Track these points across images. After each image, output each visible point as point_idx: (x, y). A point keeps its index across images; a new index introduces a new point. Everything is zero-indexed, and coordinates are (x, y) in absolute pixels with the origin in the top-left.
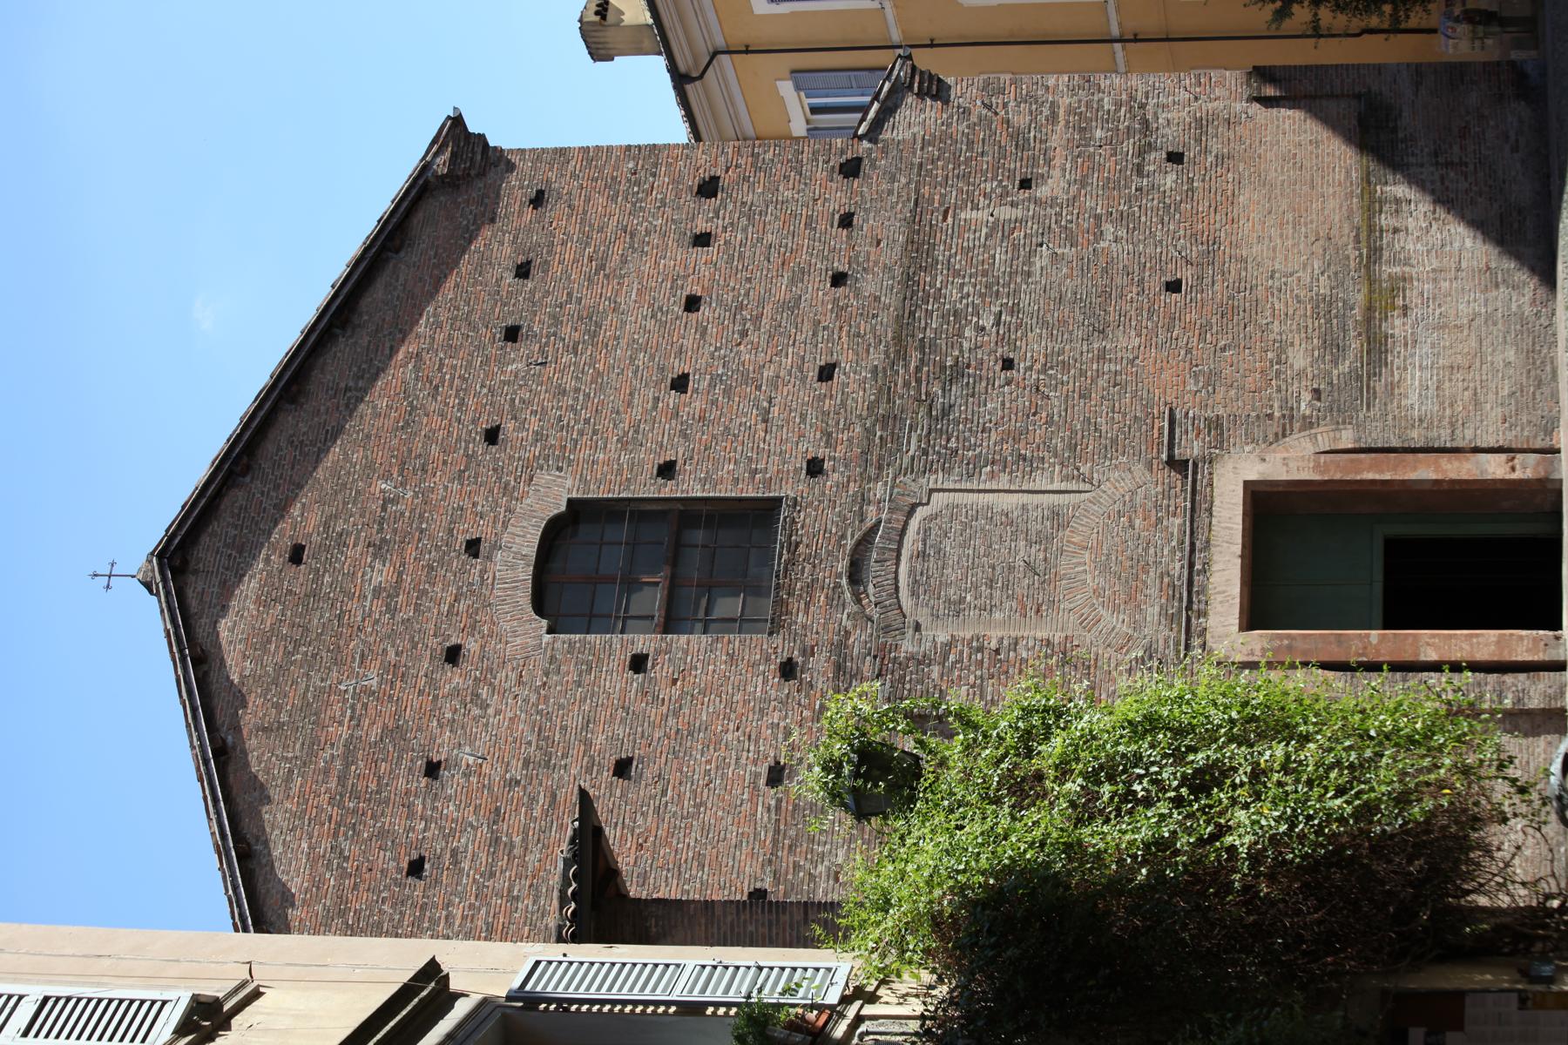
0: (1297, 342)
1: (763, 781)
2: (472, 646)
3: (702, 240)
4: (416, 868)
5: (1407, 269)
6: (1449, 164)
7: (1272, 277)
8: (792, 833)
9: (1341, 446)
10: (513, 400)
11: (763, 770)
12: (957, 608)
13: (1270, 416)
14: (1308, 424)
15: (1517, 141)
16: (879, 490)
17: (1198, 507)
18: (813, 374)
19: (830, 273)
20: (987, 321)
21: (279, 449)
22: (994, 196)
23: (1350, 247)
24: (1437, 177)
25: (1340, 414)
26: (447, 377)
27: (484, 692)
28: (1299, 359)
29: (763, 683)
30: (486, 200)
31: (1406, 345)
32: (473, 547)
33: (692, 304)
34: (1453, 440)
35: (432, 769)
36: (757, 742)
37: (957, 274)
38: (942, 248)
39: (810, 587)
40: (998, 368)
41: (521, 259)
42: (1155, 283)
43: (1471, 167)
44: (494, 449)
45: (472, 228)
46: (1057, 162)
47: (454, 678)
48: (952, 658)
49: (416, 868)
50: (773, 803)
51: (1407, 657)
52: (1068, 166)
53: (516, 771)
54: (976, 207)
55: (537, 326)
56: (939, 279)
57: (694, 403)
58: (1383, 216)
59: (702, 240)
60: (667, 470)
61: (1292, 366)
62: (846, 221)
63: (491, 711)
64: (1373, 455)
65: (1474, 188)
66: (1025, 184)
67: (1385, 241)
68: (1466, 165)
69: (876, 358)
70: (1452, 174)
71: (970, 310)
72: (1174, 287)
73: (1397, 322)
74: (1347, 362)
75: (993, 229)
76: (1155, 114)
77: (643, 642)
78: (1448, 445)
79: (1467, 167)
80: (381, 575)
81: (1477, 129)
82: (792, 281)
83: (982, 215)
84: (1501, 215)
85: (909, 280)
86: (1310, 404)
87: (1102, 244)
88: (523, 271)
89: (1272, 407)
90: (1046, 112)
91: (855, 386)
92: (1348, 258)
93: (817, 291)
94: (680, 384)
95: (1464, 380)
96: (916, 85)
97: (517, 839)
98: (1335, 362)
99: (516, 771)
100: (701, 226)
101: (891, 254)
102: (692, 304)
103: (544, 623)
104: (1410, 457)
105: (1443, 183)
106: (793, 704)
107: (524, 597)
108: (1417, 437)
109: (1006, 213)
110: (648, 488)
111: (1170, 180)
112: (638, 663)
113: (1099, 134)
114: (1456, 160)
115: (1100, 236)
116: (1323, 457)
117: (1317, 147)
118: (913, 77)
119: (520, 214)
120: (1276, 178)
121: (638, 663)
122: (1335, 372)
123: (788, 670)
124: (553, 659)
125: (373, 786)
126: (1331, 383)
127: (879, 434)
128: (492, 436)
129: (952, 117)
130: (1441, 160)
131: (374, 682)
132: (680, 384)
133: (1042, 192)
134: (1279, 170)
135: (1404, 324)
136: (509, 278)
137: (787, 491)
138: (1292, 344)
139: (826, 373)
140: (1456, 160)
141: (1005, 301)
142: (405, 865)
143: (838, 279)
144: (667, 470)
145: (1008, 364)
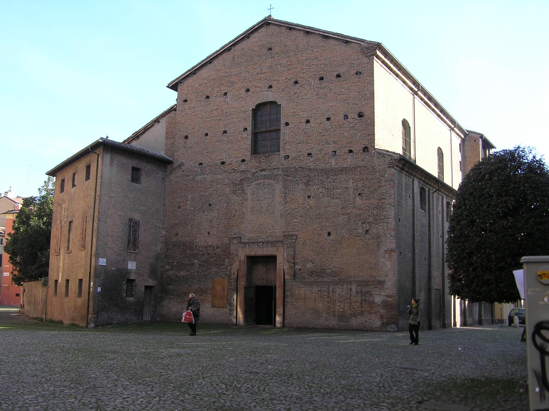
0: (313, 265)
1: (222, 161)
2: (250, 93)
3: (346, 117)
5: (331, 292)
6: (362, 304)
7: (331, 258)
8: (212, 169)
9: (285, 276)
10: (304, 84)
11: (224, 160)
12: (253, 195)
13: (294, 259)
14: (291, 267)
15: (368, 322)
17: (273, 243)
18: (309, 152)
19: (336, 150)
20: (320, 190)
21: (294, 35)
22: (357, 187)
23: (339, 277)
24: (358, 300)
25: (294, 276)
26: (311, 67)
27: (240, 99)
28: (309, 265)
30: (358, 60)
31: (311, 291)
32: (271, 87)
33: (328, 119)
34: (287, 302)
35: (226, 94)
36: (229, 158)
37: (334, 181)
38: (341, 176)
39: (260, 162)
40: (309, 194)
41: (341, 75)
42: (329, 230)
43: (361, 309)
44: (293, 84)
45: (350, 59)
46: (367, 202)
48: (243, 195)
50: (218, 164)
51: (239, 289)
52: (365, 205)
53: (225, 111)
54: (353, 183)
55: (324, 84)
56: (333, 177)
58: (347, 286)
59: (346, 117)
60: (287, 124)
61: (307, 263)
62: (351, 151)
63: (236, 102)
64: (283, 283)
65: (354, 310)
67: (339, 286)
68: (362, 308)
70: (358, 304)
71: (324, 186)
72: (329, 234)
73: (317, 289)
74: (308, 277)
75: (347, 188)
76: (381, 226)
77: (250, 129)
78: (286, 301)
79: (361, 308)
81: (372, 311)
82: (333, 141)
83: (351, 185)
84: (346, 316)
86: (297, 268)
87: (341, 216)
88: (338, 76)
89: (297, 259)
90: (383, 197)
91: (309, 163)
92: (336, 277)
94: (308, 122)
95: (302, 305)
96: (391, 162)
97: (212, 115)
98: (308, 274)
99: (225, 111)
100: (349, 117)
102: (328, 119)
103: (254, 108)
104: (282, 291)
105: (356, 301)
106: (237, 163)
107: (259, 102)
108: (288, 293)
109: (351, 191)
110: (283, 121)
111: (361, 231)
112: (246, 129)
113: (375, 212)
114: (363, 306)
116: (282, 272)
117: (369, 269)
118: (394, 160)
119: (355, 70)
120: (360, 258)
121: (246, 129)
122: (305, 274)
123: (243, 161)
124: (246, 111)
125: (222, 83)
126: (302, 273)
127: (293, 170)
128: (296, 82)
129: (382, 172)
130: (363, 301)
131: (243, 76)
132: (308, 122)
133: (358, 199)
134: (363, 259)
135: (316, 291)
136: (336, 73)
137: (281, 152)
138: (313, 264)
140: (363, 306)
141: (326, 194)
142: (208, 95)
144: (287, 124)
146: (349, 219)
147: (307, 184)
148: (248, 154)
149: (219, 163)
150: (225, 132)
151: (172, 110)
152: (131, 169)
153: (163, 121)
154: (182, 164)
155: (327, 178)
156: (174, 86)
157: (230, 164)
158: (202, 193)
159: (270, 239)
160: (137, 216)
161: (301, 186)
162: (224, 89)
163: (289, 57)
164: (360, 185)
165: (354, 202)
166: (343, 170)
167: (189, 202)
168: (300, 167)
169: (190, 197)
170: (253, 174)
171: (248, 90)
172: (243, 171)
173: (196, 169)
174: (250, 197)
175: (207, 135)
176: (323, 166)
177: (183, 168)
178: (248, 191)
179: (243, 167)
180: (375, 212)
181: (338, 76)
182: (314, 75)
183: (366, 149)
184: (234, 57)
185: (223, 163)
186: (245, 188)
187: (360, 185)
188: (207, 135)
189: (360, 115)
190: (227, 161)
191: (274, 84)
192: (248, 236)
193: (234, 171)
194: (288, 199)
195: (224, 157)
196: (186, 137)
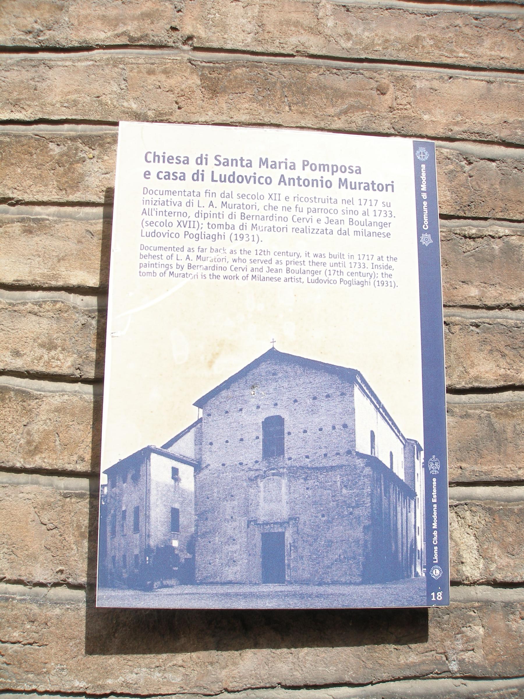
2: (260, 410)
3: (334, 428)
4: (227, 412)
12: (265, 487)
16: (285, 470)
20: (316, 484)
29: (255, 459)
32: (276, 404)
47: (254, 408)
49: (227, 412)
53: (241, 423)
57: (302, 435)
59: (334, 428)
60: (289, 433)
62: (338, 454)
66: (345, 486)
69: (309, 466)
77: (261, 437)
80: (271, 391)
85: (325, 468)
93: (324, 451)
94: (305, 432)
99: (241, 423)
100: (336, 427)
101: (331, 463)
102: (321, 430)
109: (339, 483)
110: (286, 431)
113: (357, 499)
115: (333, 501)
121: (257, 438)
123: (257, 462)
128: (296, 401)
132: (305, 432)
136: (326, 394)
137: (286, 455)
139: (307, 457)
143: (325, 455)
145: (307, 489)
146: (337, 505)
147: (305, 479)
148: (260, 457)
149: (237, 463)
150: (242, 440)
151: (200, 420)
152: (171, 469)
153: (193, 430)
154: (209, 465)
155: (321, 474)
156: (200, 403)
157: (247, 465)
158: (226, 487)
159: (279, 520)
160: (177, 506)
161: (302, 481)
162: (239, 406)
163: (289, 381)
164: (345, 479)
165: (341, 492)
166: (332, 468)
167: (215, 495)
168: (300, 466)
169: (216, 490)
170: (265, 471)
171: (258, 407)
172: (256, 470)
173: (220, 469)
174: (262, 489)
175: (227, 442)
176: (317, 465)
177: (209, 468)
178: (261, 485)
179: (257, 466)
180: (357, 499)
181: (328, 396)
182: (310, 395)
183: (349, 452)
184: (246, 381)
185: (241, 464)
186: (259, 483)
187: (345, 479)
188: (227, 442)
189: (345, 426)
190: (245, 463)
191: (279, 402)
192: (262, 519)
193: (250, 470)
194: (292, 491)
195: (241, 459)
196: (211, 444)
